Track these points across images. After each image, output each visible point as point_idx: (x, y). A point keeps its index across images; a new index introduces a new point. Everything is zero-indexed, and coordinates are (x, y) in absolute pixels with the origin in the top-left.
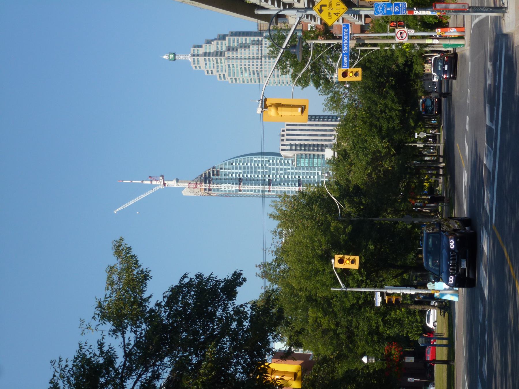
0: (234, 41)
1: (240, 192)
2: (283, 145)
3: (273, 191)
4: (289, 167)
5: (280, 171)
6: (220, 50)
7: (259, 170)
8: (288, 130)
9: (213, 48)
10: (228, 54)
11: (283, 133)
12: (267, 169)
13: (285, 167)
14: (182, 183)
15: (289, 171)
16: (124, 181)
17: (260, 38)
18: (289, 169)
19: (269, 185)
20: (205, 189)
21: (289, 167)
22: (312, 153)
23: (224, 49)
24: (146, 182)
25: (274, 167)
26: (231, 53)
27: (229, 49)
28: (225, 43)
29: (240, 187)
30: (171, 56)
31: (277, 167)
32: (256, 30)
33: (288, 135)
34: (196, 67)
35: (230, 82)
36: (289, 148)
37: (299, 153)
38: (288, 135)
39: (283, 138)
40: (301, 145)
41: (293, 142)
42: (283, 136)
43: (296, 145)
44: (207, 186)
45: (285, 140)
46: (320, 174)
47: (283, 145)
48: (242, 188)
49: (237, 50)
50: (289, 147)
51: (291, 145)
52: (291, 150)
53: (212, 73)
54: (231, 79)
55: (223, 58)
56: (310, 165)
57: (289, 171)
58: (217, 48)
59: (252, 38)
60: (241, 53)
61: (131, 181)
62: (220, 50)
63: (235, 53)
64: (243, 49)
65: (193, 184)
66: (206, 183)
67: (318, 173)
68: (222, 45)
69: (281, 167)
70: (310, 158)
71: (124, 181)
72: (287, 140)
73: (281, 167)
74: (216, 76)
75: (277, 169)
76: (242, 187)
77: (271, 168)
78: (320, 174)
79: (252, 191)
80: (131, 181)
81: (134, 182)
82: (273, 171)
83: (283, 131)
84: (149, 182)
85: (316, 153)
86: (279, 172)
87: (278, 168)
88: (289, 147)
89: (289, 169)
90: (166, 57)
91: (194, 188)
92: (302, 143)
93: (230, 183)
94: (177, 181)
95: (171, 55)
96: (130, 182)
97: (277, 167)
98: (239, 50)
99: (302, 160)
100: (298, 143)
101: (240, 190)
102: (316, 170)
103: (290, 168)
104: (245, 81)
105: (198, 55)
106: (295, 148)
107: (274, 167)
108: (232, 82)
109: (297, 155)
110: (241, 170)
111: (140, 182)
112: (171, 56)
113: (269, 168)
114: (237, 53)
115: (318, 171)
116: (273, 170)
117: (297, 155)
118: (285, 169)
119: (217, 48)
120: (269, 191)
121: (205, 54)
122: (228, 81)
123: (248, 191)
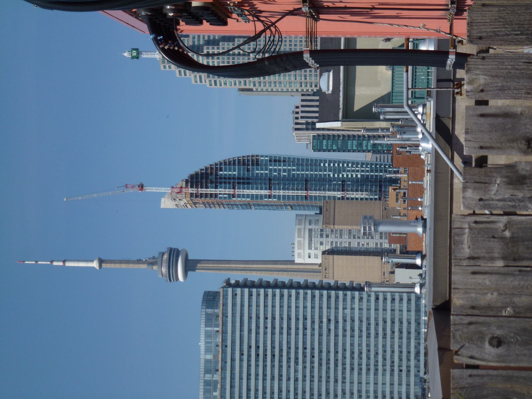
1: (233, 199)
2: (297, 124)
3: (275, 197)
4: (294, 168)
5: (283, 172)
6: (196, 43)
7: (257, 172)
8: (302, 106)
10: (208, 48)
11: (297, 110)
12: (267, 171)
13: (289, 168)
14: (107, 263)
15: (293, 172)
16: (26, 262)
18: (294, 170)
19: (269, 190)
20: (192, 194)
21: (294, 168)
24: (55, 263)
25: (275, 167)
26: (210, 47)
29: (235, 192)
30: (134, 53)
31: (279, 168)
33: (302, 112)
34: (165, 67)
35: (208, 85)
36: (305, 127)
38: (302, 112)
39: (297, 115)
41: (310, 120)
42: (297, 113)
44: (194, 191)
45: (300, 118)
46: (332, 176)
47: (297, 124)
48: (237, 193)
49: (218, 45)
50: (304, 126)
51: (307, 123)
52: (307, 129)
53: (185, 75)
54: (209, 80)
56: (329, 148)
57: (293, 172)
58: (194, 42)
61: (36, 262)
62: (196, 43)
63: (216, 47)
64: (226, 43)
65: (178, 188)
66: (192, 187)
67: (329, 175)
68: (200, 38)
69: (284, 168)
70: (329, 139)
71: (26, 262)
72: (302, 117)
73: (284, 168)
74: (191, 78)
75: (280, 170)
77: (271, 169)
78: (332, 176)
79: (248, 196)
80: (36, 262)
81: (39, 263)
82: (274, 172)
83: (297, 107)
84: (61, 264)
86: (282, 174)
87: (281, 169)
88: (304, 126)
89: (294, 170)
90: (126, 54)
91: (178, 193)
93: (222, 188)
95: (133, 52)
96: (34, 262)
97: (279, 168)
98: (221, 43)
101: (234, 196)
102: (327, 172)
103: (295, 169)
104: (228, 84)
106: (312, 127)
107: (275, 167)
108: (211, 85)
109: (314, 136)
110: (236, 171)
111: (49, 263)
112: (134, 53)
113: (270, 169)
114: (218, 48)
115: (329, 173)
116: (275, 172)
117: (314, 136)
118: (289, 170)
119: (194, 42)
120: (270, 197)
122: (206, 85)
123: (244, 196)
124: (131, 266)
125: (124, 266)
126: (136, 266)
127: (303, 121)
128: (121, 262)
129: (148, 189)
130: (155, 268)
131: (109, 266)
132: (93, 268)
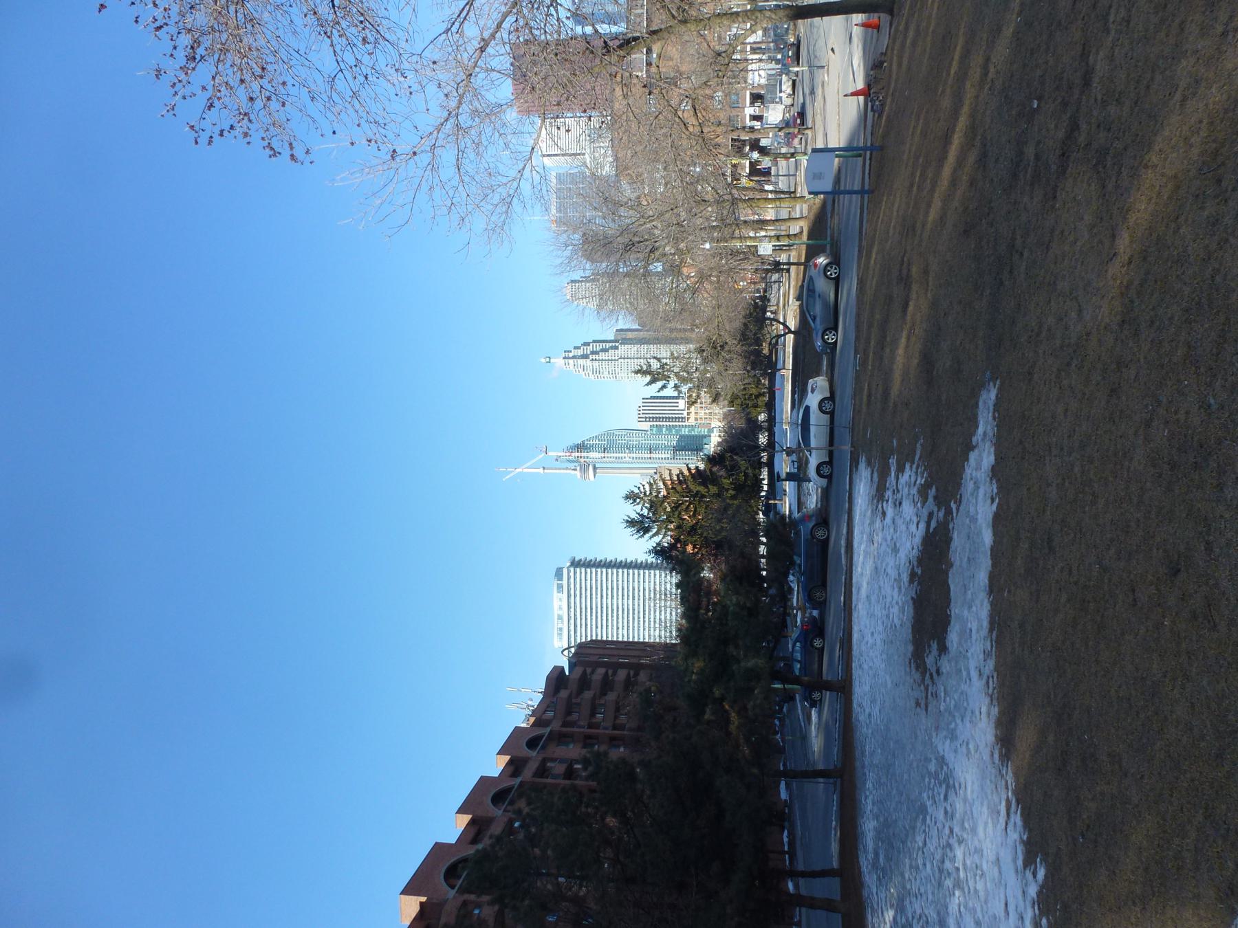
0: (599, 347)
9: (580, 352)
17: (617, 344)
22: (661, 423)
23: (589, 353)
27: (593, 353)
28: (590, 348)
32: (612, 338)
37: (652, 423)
40: (653, 418)
41: (647, 416)
43: (650, 418)
51: (646, 418)
55: (588, 360)
59: (611, 344)
60: (602, 356)
76: (606, 455)
85: (665, 423)
90: (543, 360)
92: (654, 416)
94: (544, 468)
99: (655, 429)
100: (651, 416)
105: (569, 358)
121: (574, 357)
124: (562, 471)
125: (558, 471)
126: (565, 471)
127: (644, 416)
128: (556, 469)
129: (550, 454)
130: (575, 472)
131: (548, 471)
132: (539, 473)
